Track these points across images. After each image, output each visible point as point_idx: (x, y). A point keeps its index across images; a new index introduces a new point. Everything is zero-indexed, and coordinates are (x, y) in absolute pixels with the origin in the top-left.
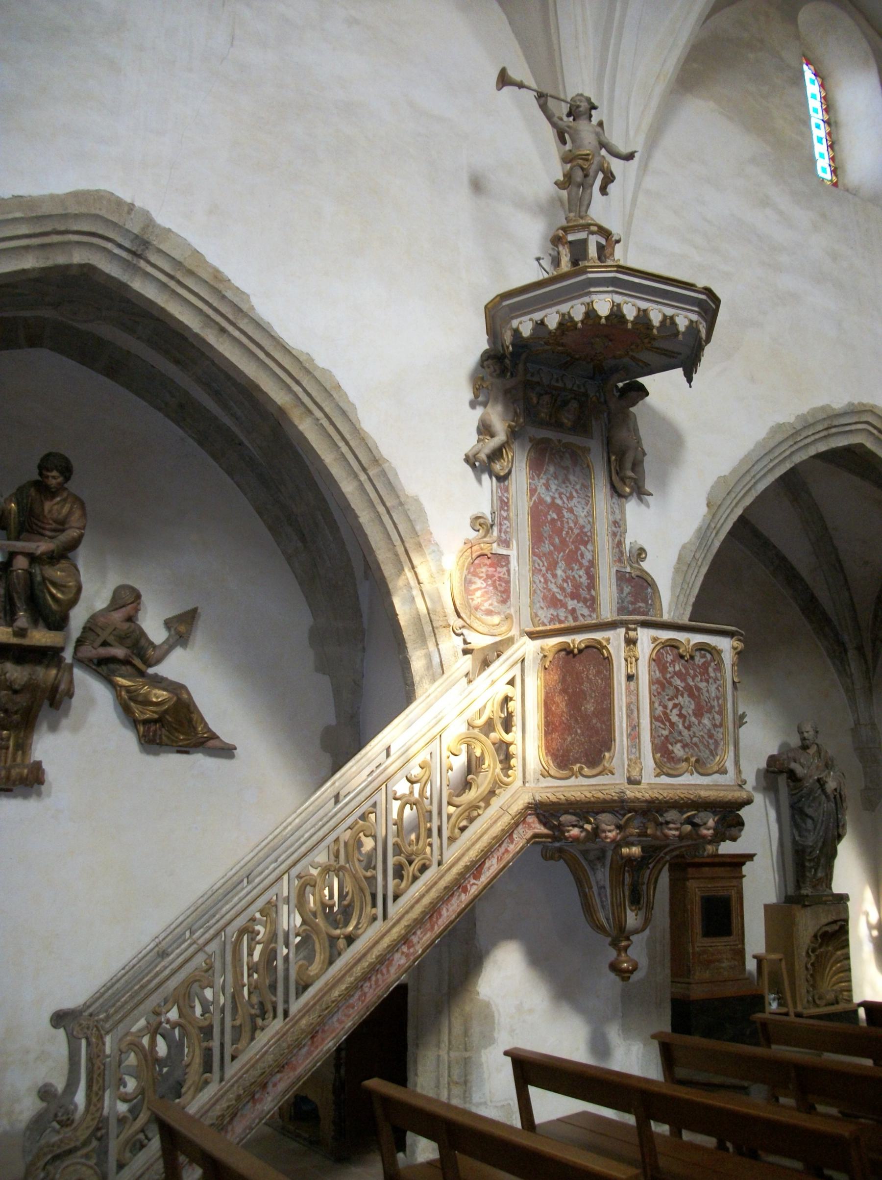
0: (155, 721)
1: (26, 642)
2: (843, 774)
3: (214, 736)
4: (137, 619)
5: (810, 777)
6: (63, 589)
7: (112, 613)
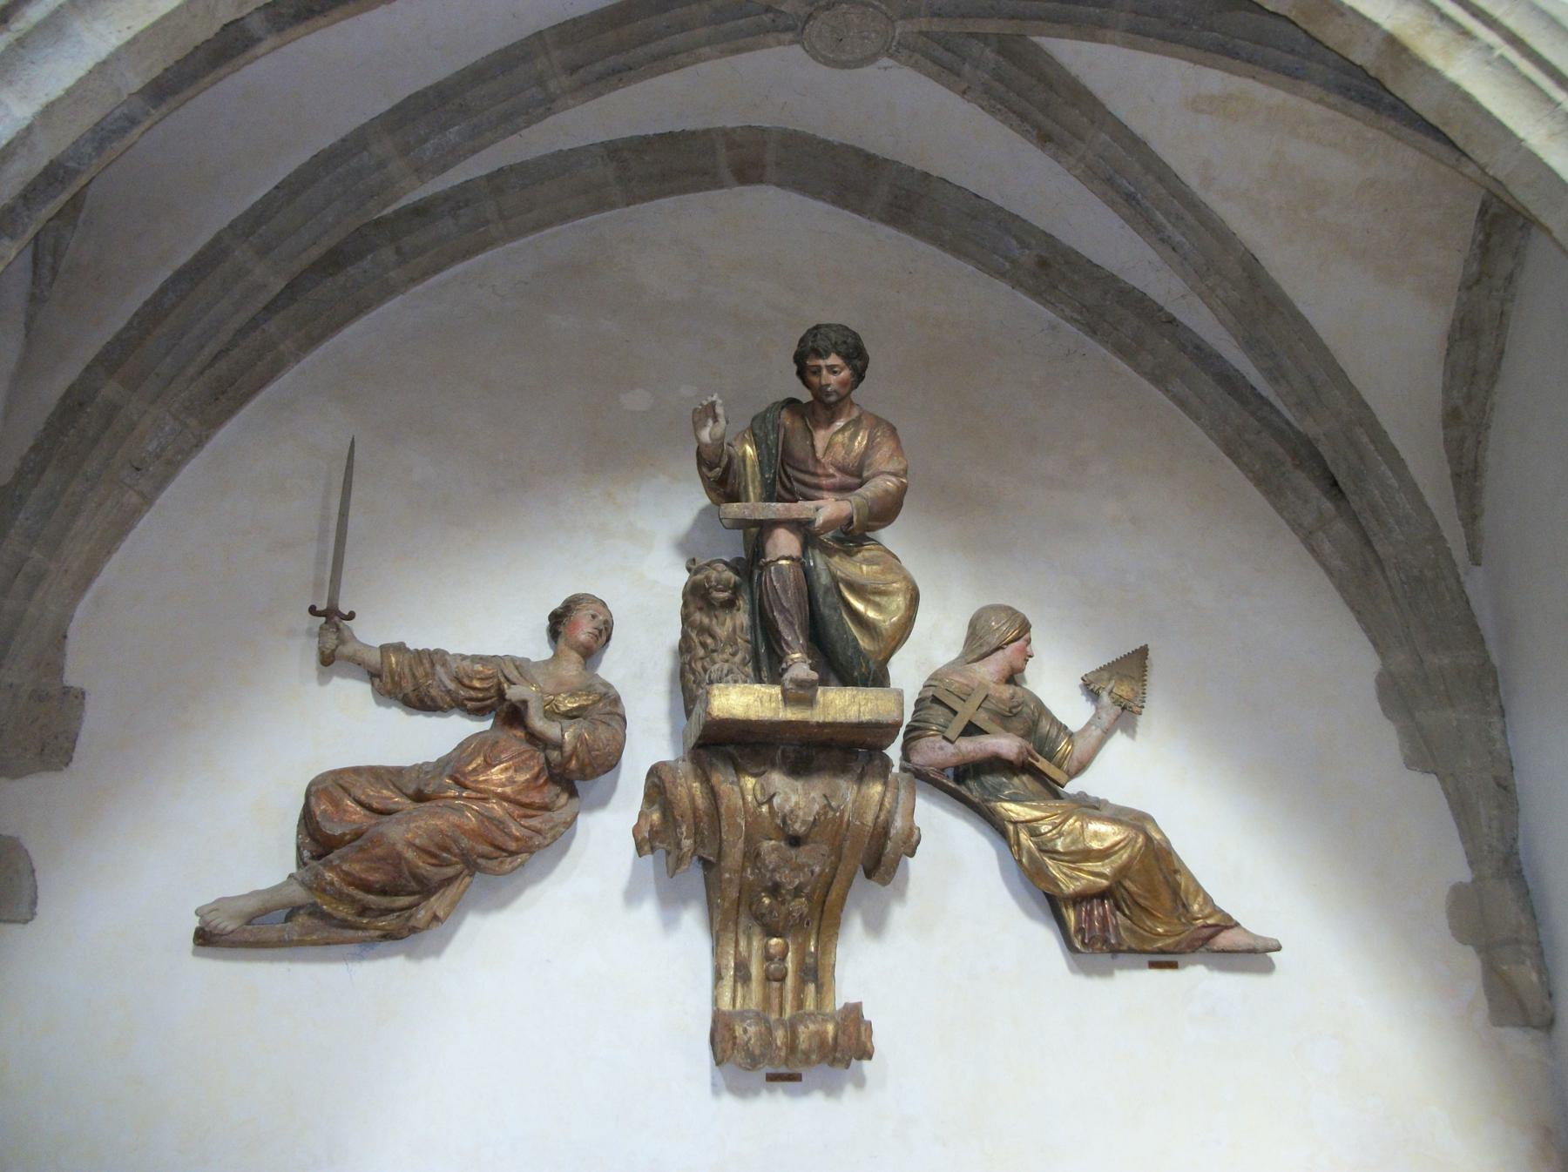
0: (1102, 895)
1: (816, 715)
3: (1228, 924)
4: (1024, 680)
6: (882, 600)
7: (976, 666)
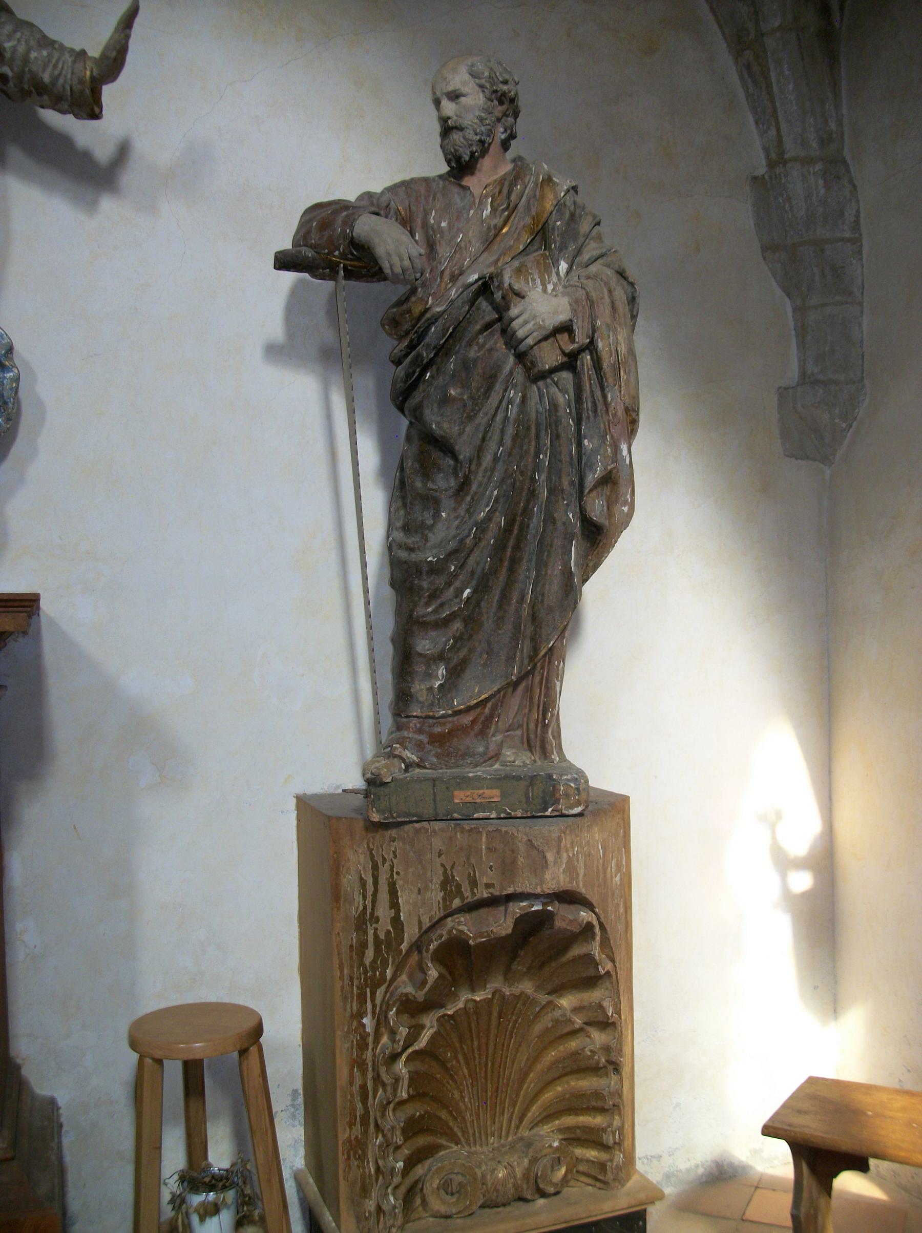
2: (621, 274)
5: (454, 278)
